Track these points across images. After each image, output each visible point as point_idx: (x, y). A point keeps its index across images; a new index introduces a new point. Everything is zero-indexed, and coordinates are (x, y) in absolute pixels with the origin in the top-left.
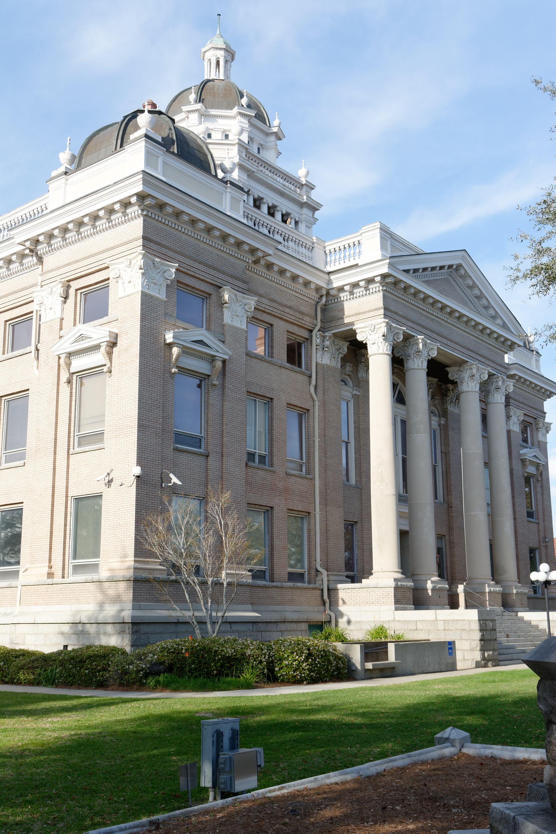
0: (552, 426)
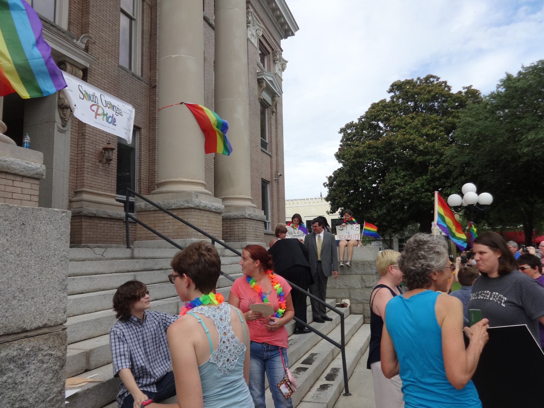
0: (287, 64)
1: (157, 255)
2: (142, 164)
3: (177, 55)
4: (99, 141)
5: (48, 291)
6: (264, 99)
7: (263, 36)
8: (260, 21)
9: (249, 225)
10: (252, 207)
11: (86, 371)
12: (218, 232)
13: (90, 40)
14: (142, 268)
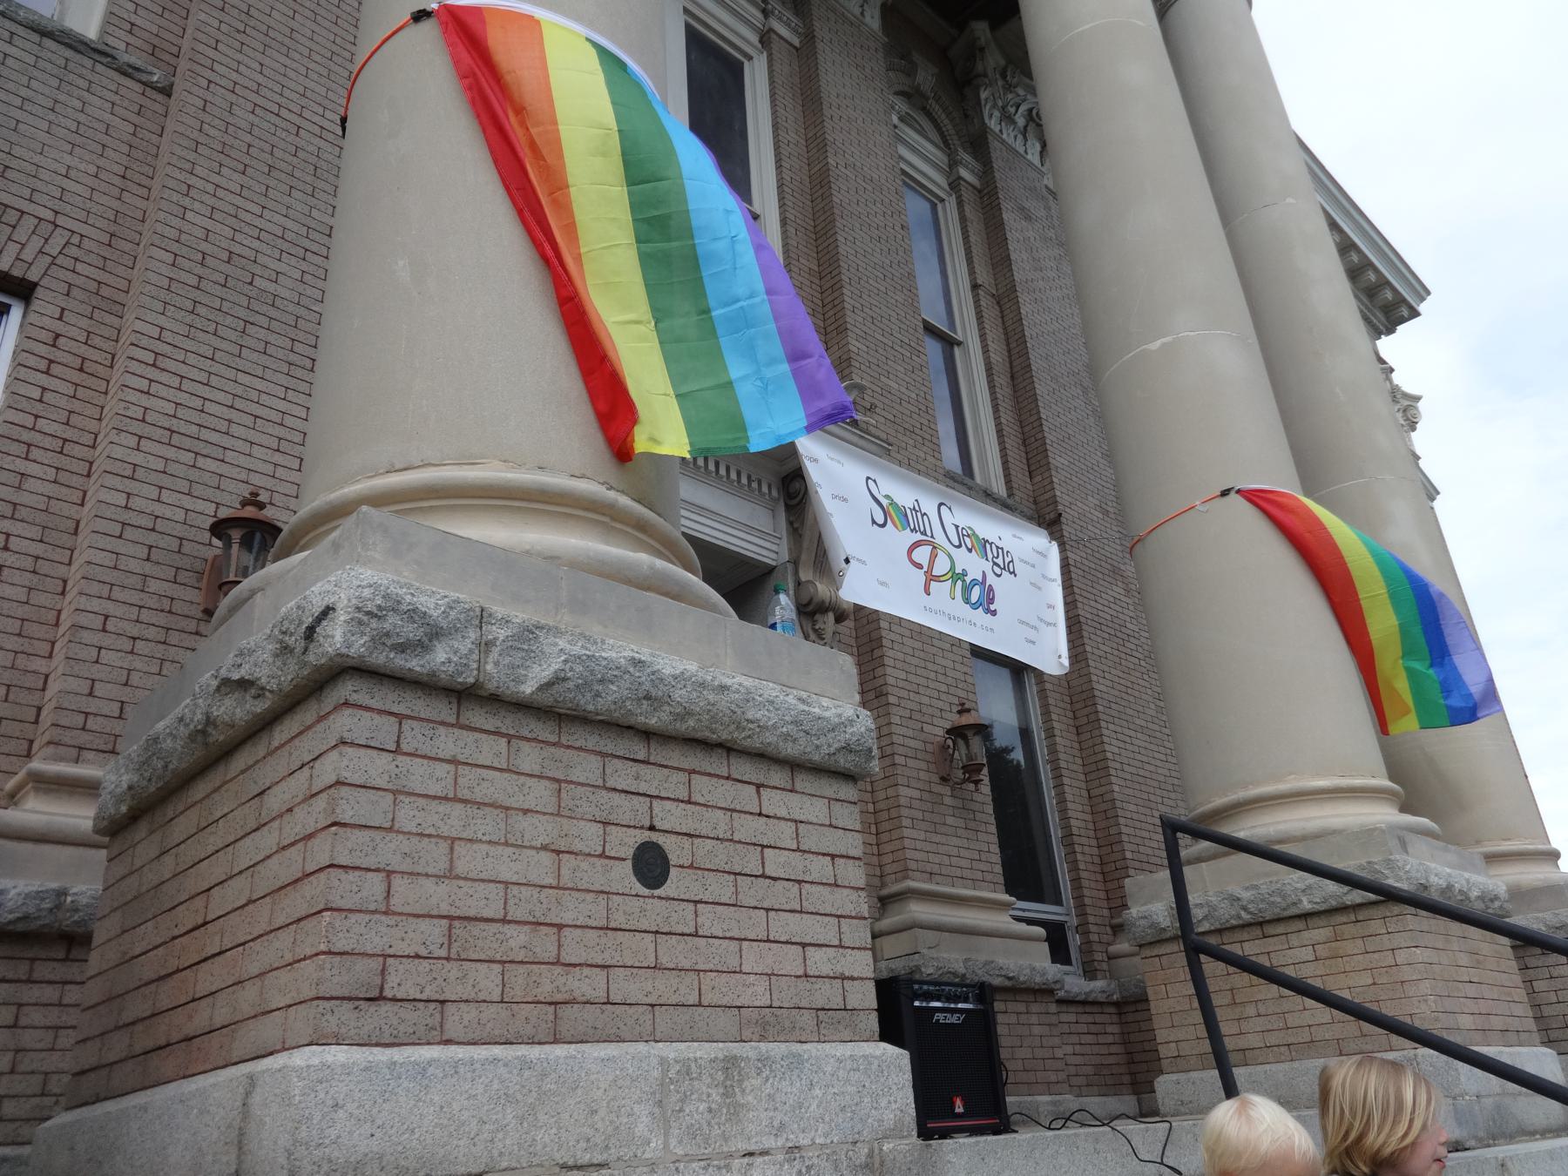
2: (1066, 781)
3: (1169, 339)
4: (930, 710)
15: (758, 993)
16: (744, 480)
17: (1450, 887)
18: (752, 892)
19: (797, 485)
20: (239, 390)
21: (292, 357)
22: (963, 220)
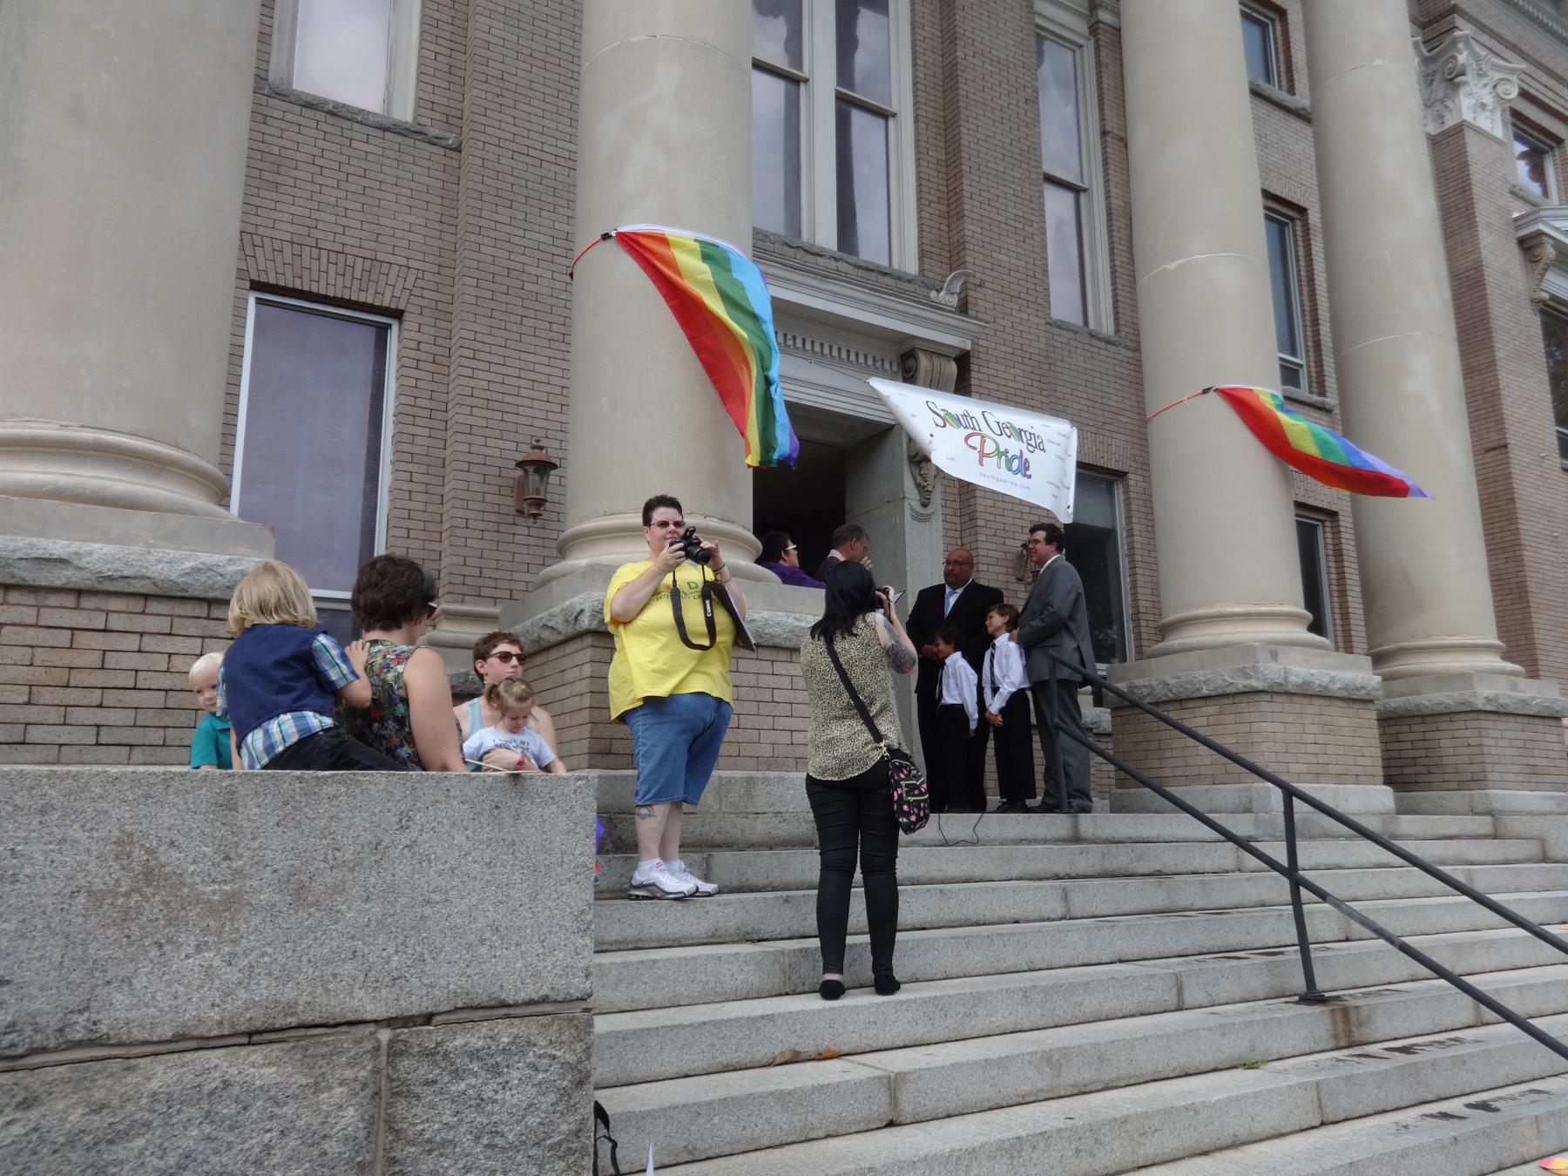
1: (1153, 833)
3: (1182, 261)
5: (550, 932)
6: (1554, 298)
7: (1524, 94)
8: (1508, 53)
9: (1492, 733)
10: (1503, 672)
11: (891, 1124)
12: (1367, 761)
13: (971, 279)
14: (1098, 868)
15: (767, 751)
16: (870, 362)
17: (1305, 683)
18: (765, 709)
19: (910, 362)
20: (522, 365)
21: (551, 335)
22: (1099, 65)
